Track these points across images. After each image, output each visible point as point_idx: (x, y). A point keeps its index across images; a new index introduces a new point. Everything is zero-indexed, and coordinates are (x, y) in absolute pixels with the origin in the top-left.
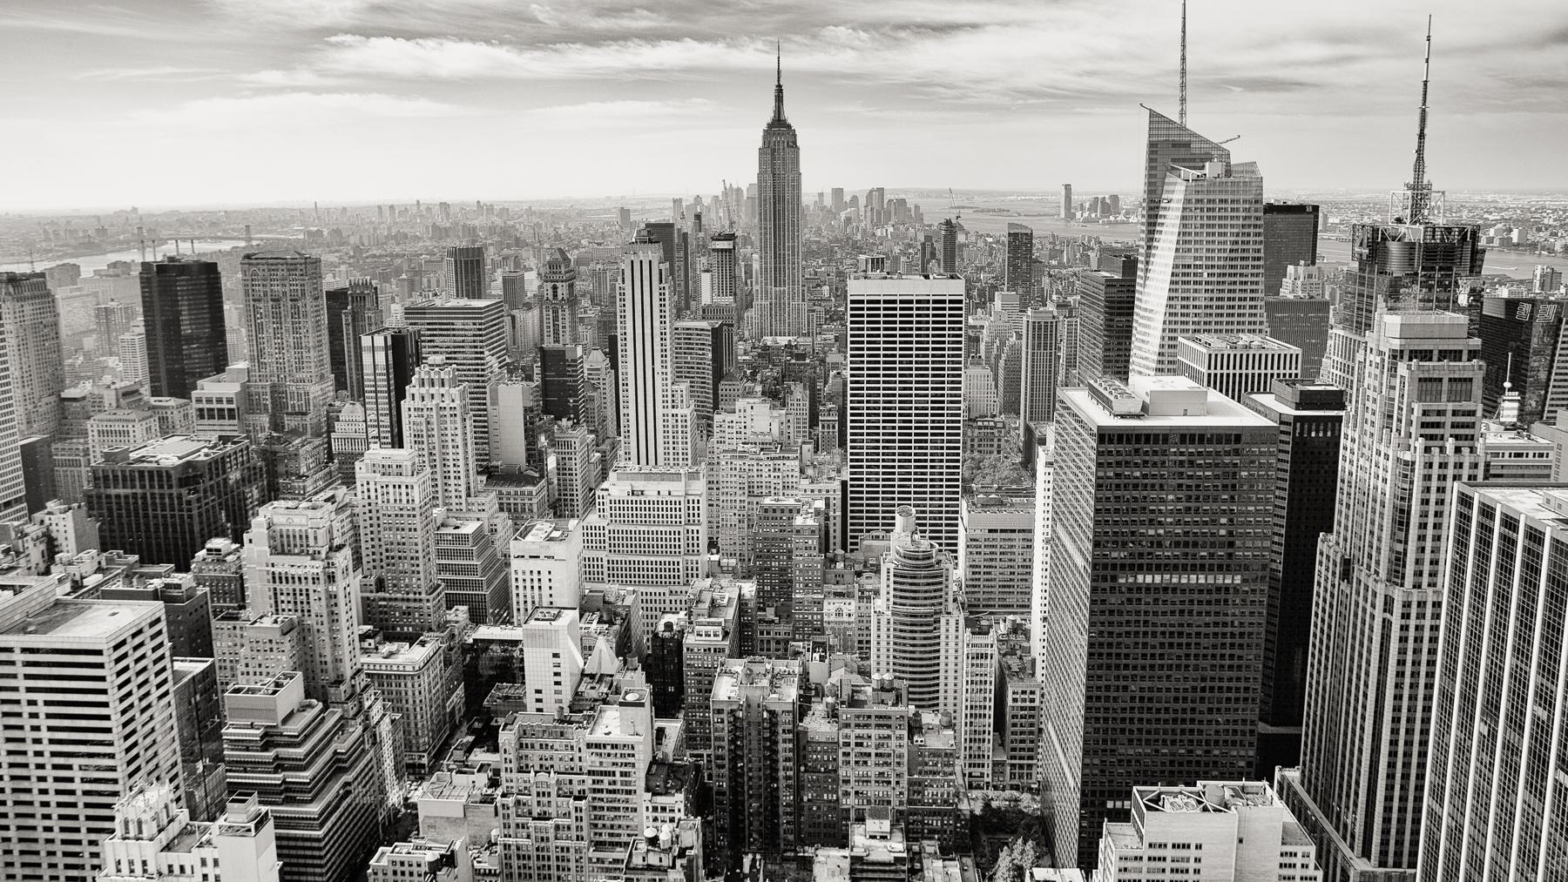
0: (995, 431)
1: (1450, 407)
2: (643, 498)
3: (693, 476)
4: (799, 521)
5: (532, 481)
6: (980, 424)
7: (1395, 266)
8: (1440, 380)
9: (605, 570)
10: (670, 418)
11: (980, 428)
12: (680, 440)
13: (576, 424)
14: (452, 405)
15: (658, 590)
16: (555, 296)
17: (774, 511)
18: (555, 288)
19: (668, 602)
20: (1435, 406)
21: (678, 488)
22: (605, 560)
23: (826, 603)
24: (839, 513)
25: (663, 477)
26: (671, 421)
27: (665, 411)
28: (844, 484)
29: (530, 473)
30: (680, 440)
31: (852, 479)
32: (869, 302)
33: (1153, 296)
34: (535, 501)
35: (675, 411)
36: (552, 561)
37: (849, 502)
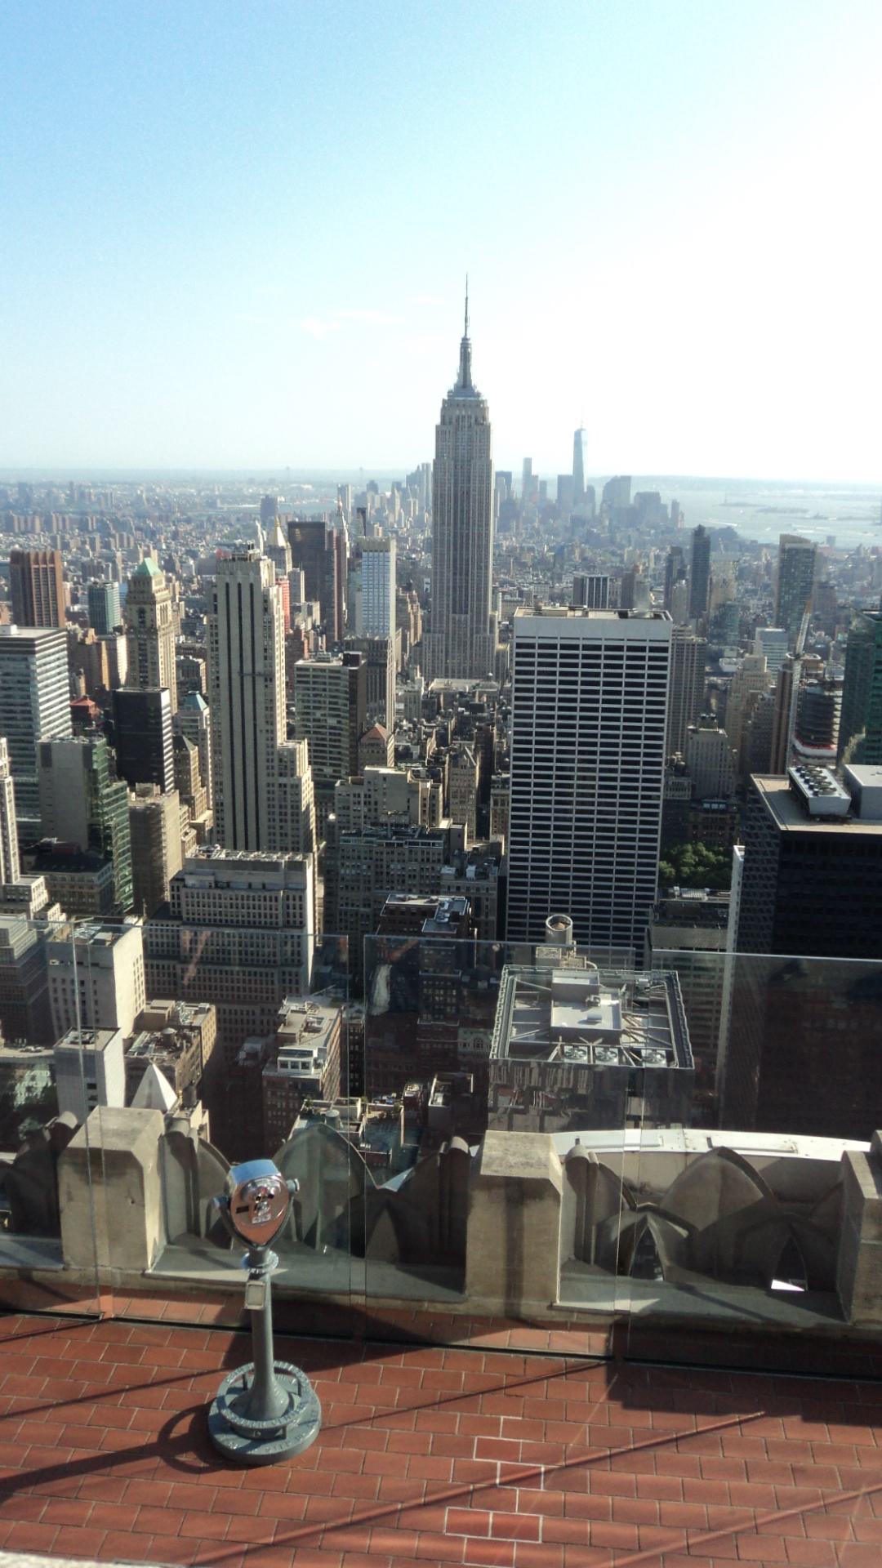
0: (728, 816)
2: (230, 893)
6: (706, 806)
10: (276, 789)
11: (707, 811)
12: (289, 817)
15: (245, 1008)
17: (403, 913)
18: (142, 612)
19: (258, 1022)
23: (461, 1031)
24: (493, 918)
28: (502, 881)
30: (289, 817)
31: (512, 875)
35: (283, 780)
36: (97, 969)
37: (508, 904)
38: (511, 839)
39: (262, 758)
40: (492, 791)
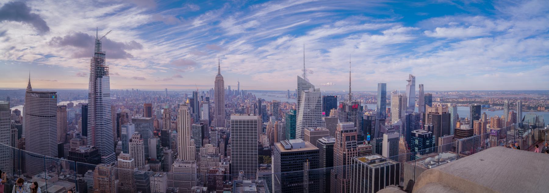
1: (352, 142)
3: (193, 163)
4: (217, 174)
5: (158, 163)
7: (347, 110)
8: (350, 136)
9: (173, 184)
10: (190, 148)
13: (169, 149)
14: (140, 144)
16: (166, 117)
17: (213, 171)
20: (349, 142)
21: (190, 165)
22: (173, 181)
24: (229, 172)
25: (187, 163)
26: (190, 149)
27: (189, 147)
29: (158, 161)
31: (232, 164)
32: (236, 121)
33: (300, 118)
34: (158, 167)
35: (191, 147)
38: (231, 157)
39: (187, 142)
40: (227, 148)
